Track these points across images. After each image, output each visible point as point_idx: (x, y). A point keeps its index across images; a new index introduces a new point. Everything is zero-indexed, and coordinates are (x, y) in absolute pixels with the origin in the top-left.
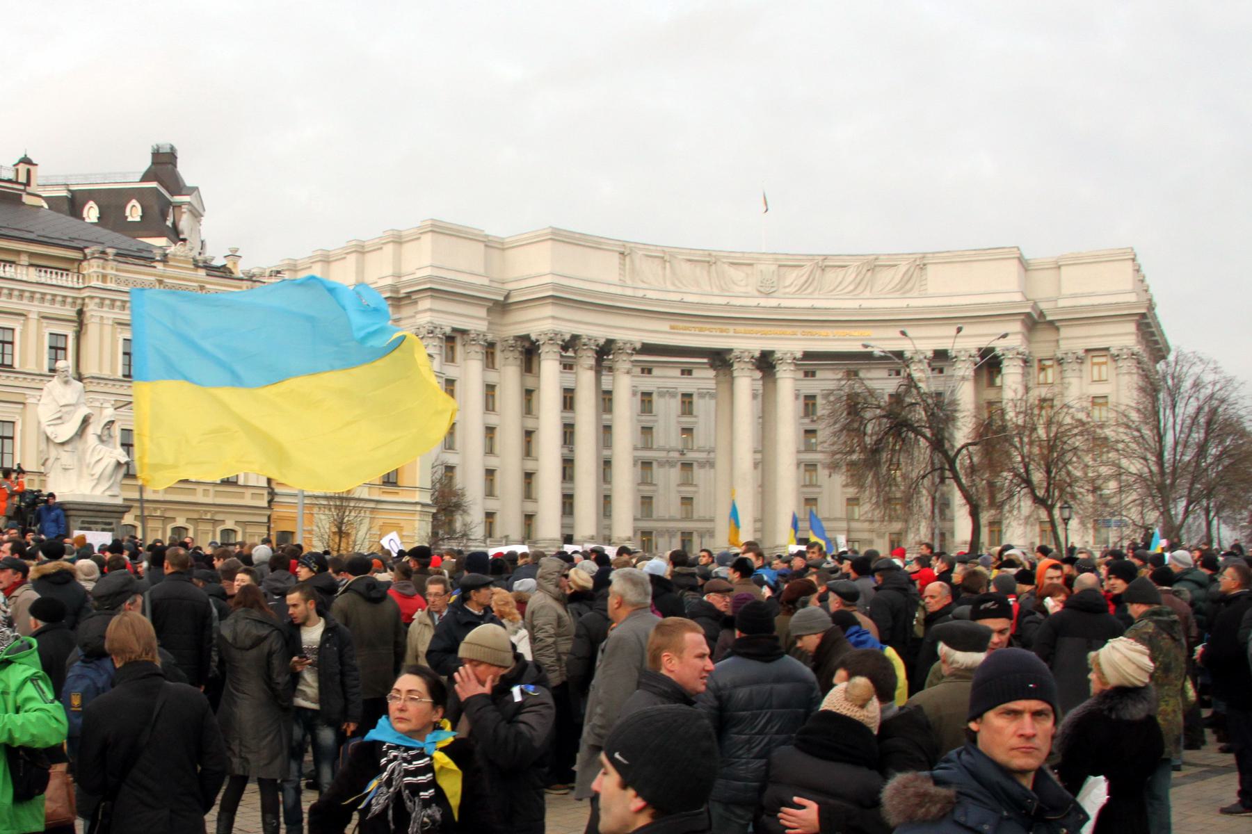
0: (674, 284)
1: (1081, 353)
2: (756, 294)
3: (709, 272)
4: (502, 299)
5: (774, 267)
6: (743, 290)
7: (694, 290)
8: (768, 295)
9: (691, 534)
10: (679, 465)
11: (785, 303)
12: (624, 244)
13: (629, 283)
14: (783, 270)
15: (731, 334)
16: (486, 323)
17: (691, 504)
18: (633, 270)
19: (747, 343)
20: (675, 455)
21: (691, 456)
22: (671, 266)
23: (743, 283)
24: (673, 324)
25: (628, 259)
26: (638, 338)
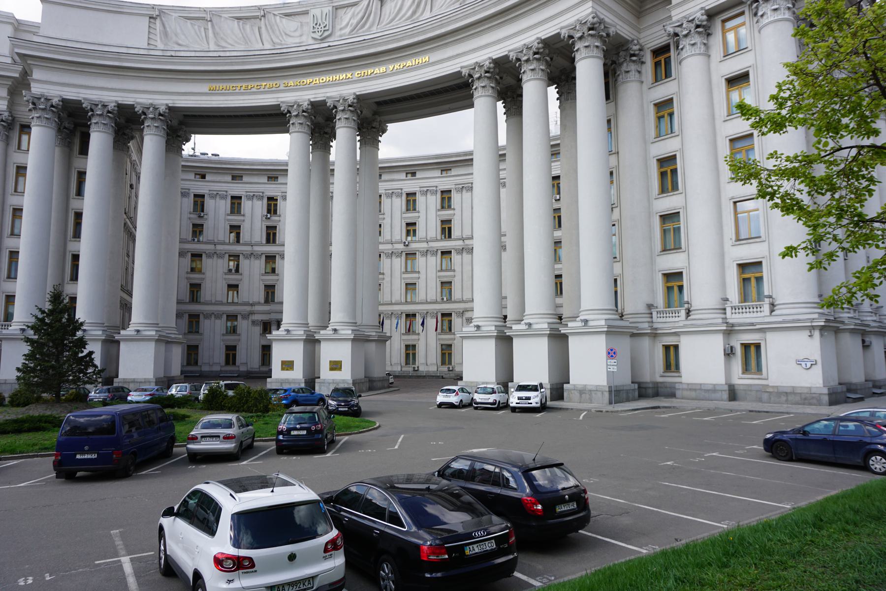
0: (219, 46)
1: (700, 16)
2: (311, 41)
3: (259, 28)
4: (17, 75)
5: (327, 9)
6: (297, 40)
7: (242, 48)
8: (323, 39)
9: (414, 315)
10: (404, 254)
11: (331, 44)
12: (153, 7)
13: (160, 46)
14: (341, 12)
15: (282, 87)
16: (6, 103)
17: (415, 289)
18: (165, 34)
19: (296, 94)
20: (401, 246)
21: (414, 246)
22: (213, 26)
23: (297, 34)
24: (214, 85)
25: (158, 21)
26: (163, 101)
